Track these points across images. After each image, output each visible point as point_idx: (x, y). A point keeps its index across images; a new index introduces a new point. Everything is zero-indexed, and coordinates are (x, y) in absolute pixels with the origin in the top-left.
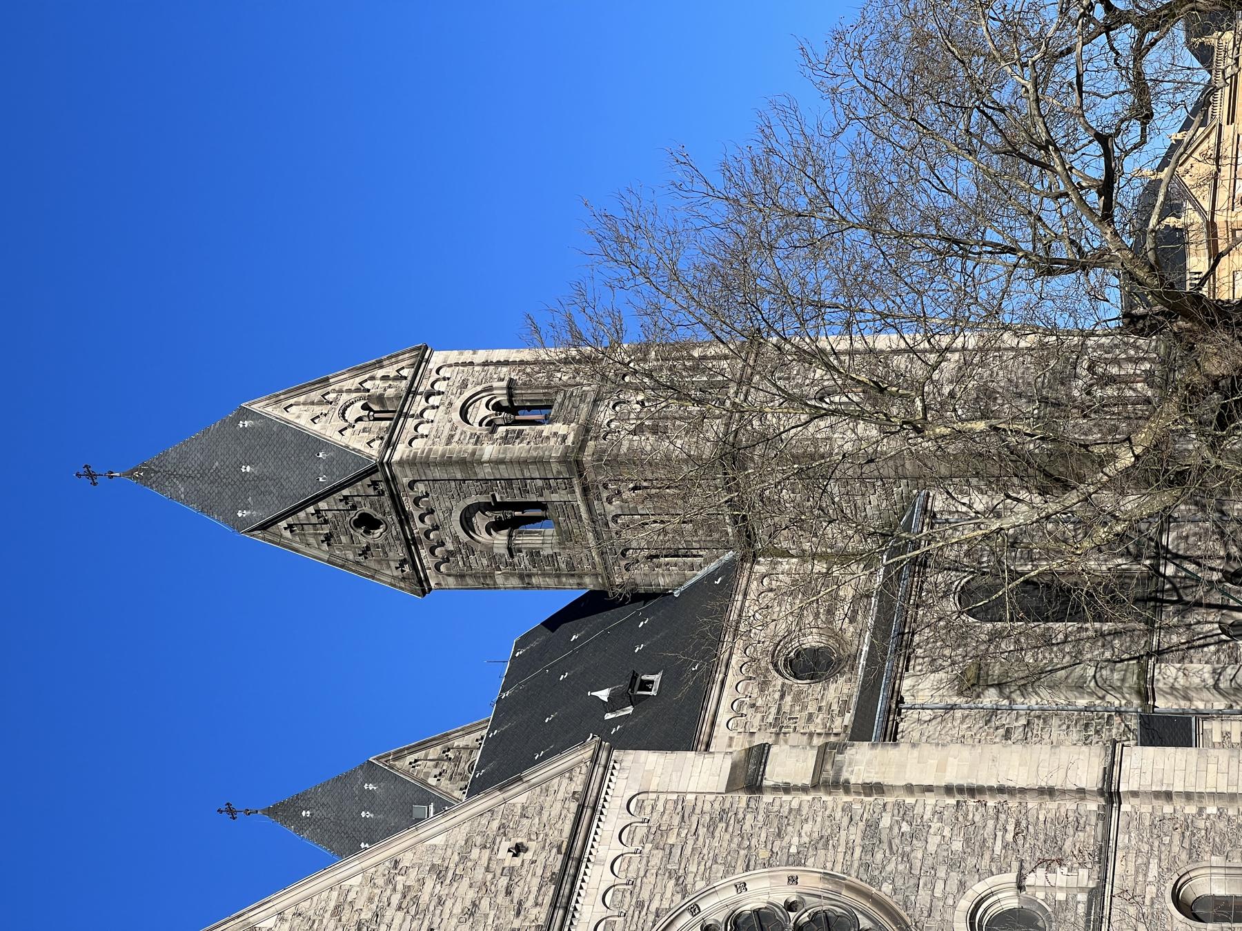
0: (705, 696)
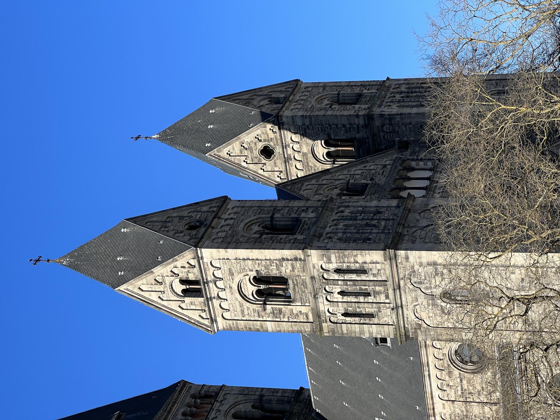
0: (424, 386)
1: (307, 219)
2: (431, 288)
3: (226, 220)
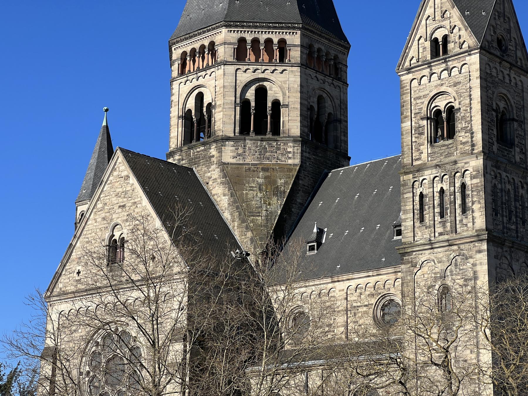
0: (359, 271)
1: (513, 154)
2: (452, 275)
3: (509, 75)
